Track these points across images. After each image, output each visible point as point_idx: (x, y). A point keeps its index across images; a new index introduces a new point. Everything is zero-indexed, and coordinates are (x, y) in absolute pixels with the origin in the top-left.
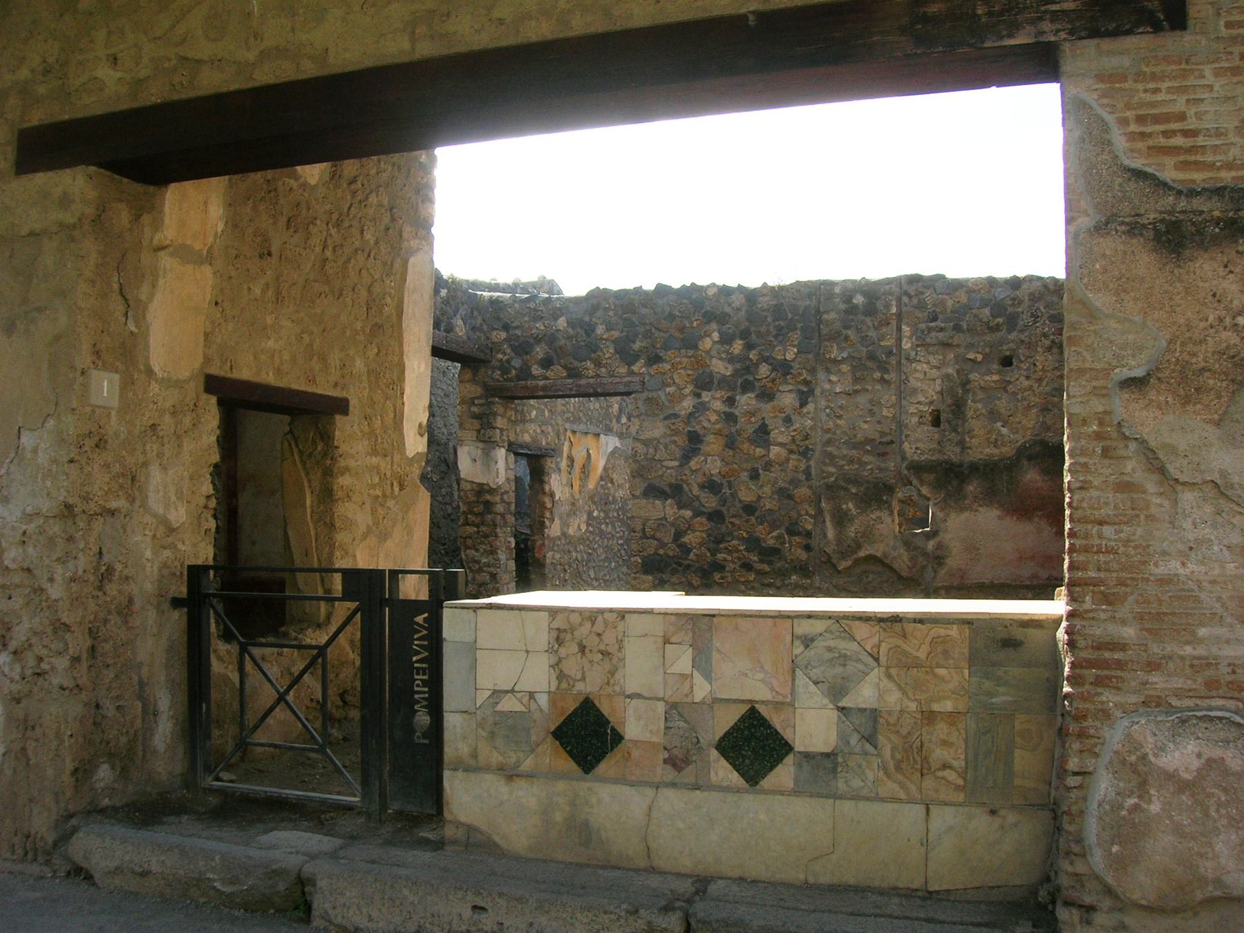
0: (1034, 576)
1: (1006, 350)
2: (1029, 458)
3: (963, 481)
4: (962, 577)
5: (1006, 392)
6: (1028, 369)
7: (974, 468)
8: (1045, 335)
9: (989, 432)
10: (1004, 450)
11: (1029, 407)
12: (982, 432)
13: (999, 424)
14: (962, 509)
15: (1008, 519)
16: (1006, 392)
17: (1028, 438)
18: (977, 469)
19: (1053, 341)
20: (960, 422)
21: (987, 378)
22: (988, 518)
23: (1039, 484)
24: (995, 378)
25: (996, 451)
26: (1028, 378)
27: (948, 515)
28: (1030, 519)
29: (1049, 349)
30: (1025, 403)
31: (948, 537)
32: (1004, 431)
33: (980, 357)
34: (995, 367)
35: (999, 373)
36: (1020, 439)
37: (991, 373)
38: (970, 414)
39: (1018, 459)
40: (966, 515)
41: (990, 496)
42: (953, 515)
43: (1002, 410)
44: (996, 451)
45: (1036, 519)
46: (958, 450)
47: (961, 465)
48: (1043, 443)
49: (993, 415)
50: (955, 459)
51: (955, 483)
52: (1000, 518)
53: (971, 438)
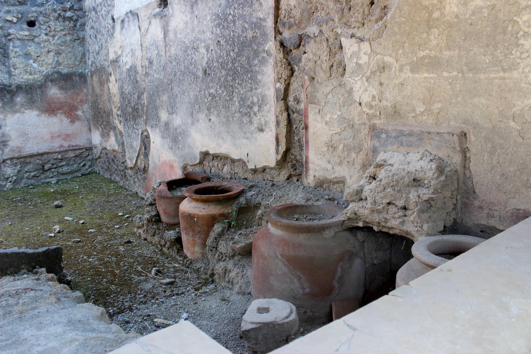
0: (61, 146)
1: (31, 17)
2: (52, 81)
3: (13, 95)
4: (20, 152)
5: (34, 42)
6: (46, 29)
7: (19, 87)
8: (55, 10)
9: (26, 66)
10: (36, 76)
11: (49, 52)
12: (21, 66)
13: (31, 61)
14: (15, 112)
15: (43, 116)
16: (34, 42)
17: (49, 69)
18: (21, 88)
19: (60, 15)
20: (6, 59)
21: (21, 33)
22: (31, 116)
23: (59, 96)
24: (27, 33)
25: (31, 77)
26: (46, 34)
27: (6, 116)
28: (55, 115)
29: (57, 19)
30: (46, 49)
31: (8, 129)
32: (35, 65)
33: (15, 20)
34: (25, 26)
35: (28, 30)
36: (46, 70)
37: (22, 30)
38: (12, 55)
39: (45, 81)
40: (18, 115)
41: (31, 103)
42: (9, 116)
43: (33, 53)
44: (31, 77)
45: (59, 115)
46: (7, 76)
47: (10, 86)
48: (58, 73)
49: (27, 55)
50: (6, 82)
51: (8, 96)
52: (38, 116)
53: (15, 69)
